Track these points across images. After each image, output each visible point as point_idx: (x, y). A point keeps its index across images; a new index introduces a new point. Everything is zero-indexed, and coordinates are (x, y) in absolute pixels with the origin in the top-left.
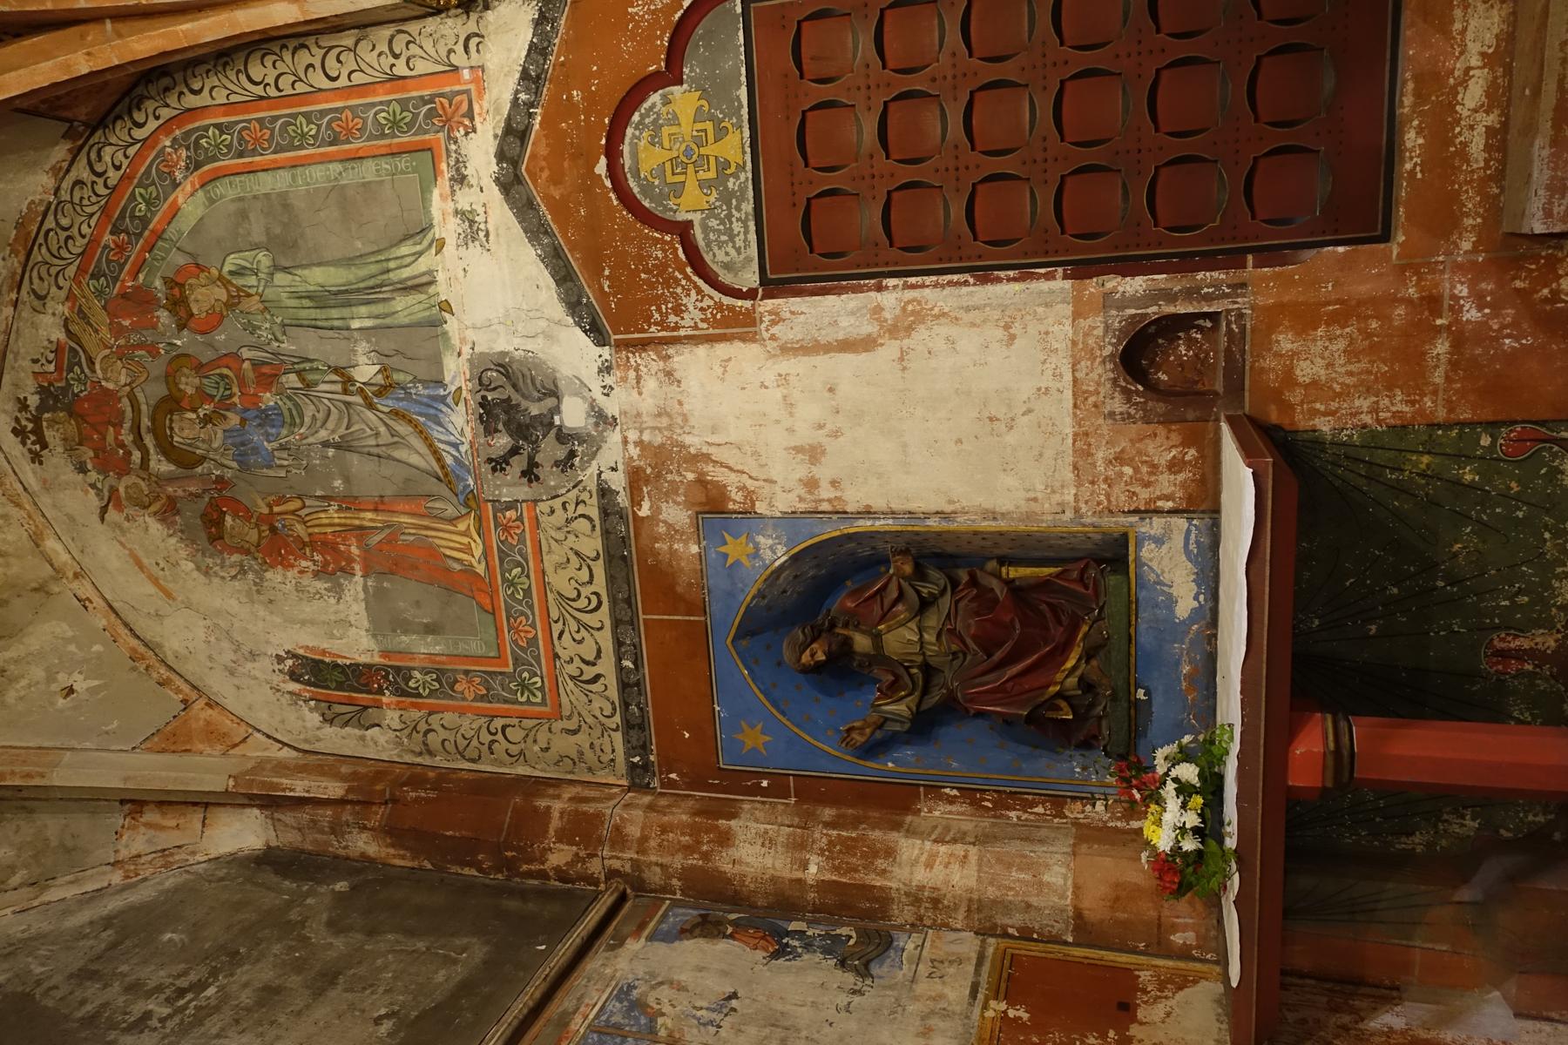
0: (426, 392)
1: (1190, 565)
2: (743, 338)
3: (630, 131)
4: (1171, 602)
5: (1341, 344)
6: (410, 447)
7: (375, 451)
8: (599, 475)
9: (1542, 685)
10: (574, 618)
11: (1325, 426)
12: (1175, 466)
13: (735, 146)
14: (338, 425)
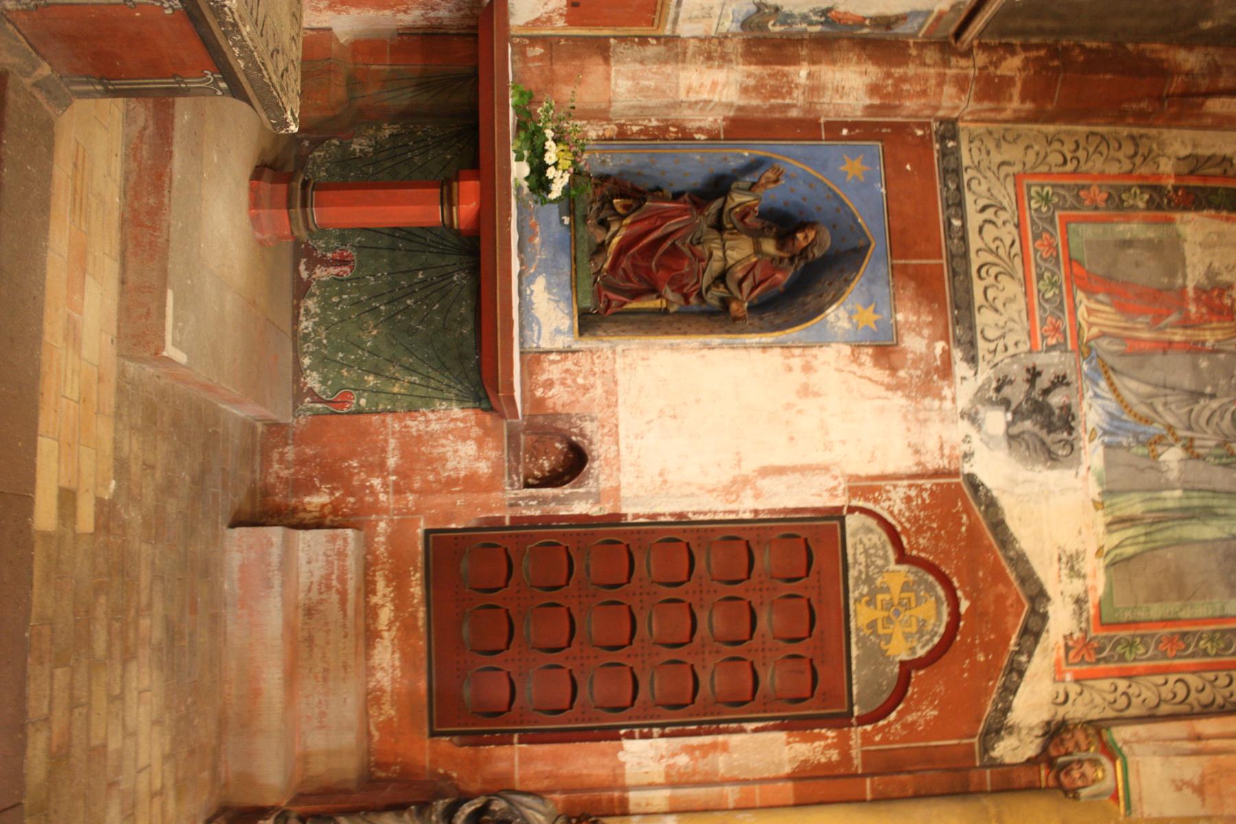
0: (1119, 439)
1: (537, 315)
2: (858, 478)
3: (942, 630)
4: (549, 288)
5: (450, 465)
6: (1137, 395)
7: (1168, 391)
8: (976, 374)
9: (321, 244)
10: (1000, 258)
11: (457, 412)
12: (549, 384)
13: (861, 616)
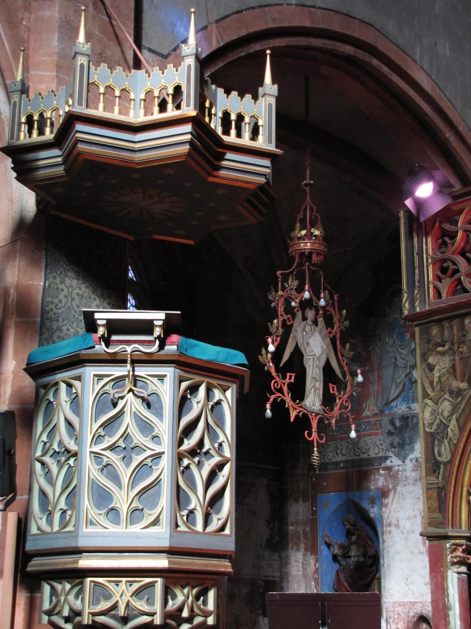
6: (396, 390)
14: (400, 362)
